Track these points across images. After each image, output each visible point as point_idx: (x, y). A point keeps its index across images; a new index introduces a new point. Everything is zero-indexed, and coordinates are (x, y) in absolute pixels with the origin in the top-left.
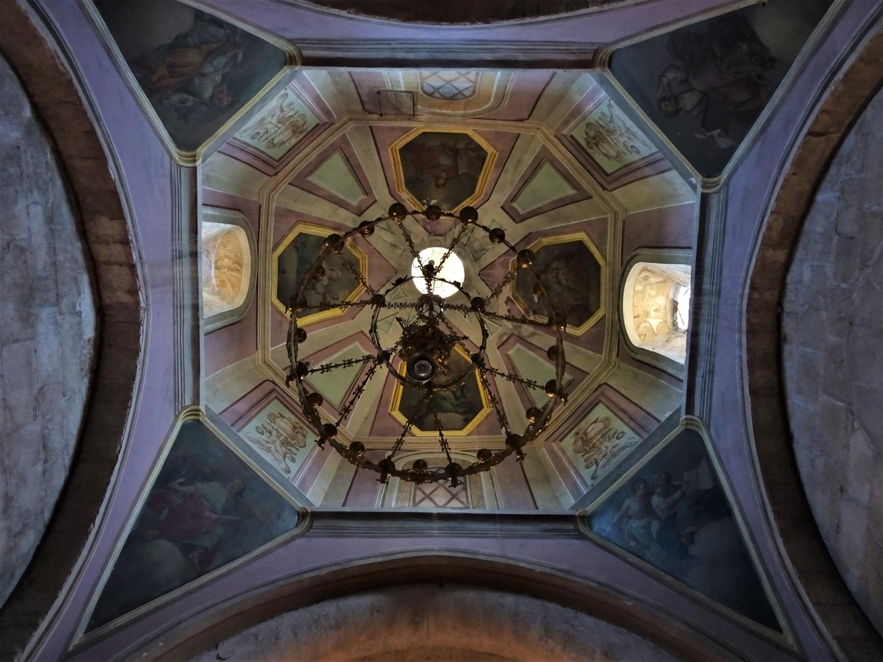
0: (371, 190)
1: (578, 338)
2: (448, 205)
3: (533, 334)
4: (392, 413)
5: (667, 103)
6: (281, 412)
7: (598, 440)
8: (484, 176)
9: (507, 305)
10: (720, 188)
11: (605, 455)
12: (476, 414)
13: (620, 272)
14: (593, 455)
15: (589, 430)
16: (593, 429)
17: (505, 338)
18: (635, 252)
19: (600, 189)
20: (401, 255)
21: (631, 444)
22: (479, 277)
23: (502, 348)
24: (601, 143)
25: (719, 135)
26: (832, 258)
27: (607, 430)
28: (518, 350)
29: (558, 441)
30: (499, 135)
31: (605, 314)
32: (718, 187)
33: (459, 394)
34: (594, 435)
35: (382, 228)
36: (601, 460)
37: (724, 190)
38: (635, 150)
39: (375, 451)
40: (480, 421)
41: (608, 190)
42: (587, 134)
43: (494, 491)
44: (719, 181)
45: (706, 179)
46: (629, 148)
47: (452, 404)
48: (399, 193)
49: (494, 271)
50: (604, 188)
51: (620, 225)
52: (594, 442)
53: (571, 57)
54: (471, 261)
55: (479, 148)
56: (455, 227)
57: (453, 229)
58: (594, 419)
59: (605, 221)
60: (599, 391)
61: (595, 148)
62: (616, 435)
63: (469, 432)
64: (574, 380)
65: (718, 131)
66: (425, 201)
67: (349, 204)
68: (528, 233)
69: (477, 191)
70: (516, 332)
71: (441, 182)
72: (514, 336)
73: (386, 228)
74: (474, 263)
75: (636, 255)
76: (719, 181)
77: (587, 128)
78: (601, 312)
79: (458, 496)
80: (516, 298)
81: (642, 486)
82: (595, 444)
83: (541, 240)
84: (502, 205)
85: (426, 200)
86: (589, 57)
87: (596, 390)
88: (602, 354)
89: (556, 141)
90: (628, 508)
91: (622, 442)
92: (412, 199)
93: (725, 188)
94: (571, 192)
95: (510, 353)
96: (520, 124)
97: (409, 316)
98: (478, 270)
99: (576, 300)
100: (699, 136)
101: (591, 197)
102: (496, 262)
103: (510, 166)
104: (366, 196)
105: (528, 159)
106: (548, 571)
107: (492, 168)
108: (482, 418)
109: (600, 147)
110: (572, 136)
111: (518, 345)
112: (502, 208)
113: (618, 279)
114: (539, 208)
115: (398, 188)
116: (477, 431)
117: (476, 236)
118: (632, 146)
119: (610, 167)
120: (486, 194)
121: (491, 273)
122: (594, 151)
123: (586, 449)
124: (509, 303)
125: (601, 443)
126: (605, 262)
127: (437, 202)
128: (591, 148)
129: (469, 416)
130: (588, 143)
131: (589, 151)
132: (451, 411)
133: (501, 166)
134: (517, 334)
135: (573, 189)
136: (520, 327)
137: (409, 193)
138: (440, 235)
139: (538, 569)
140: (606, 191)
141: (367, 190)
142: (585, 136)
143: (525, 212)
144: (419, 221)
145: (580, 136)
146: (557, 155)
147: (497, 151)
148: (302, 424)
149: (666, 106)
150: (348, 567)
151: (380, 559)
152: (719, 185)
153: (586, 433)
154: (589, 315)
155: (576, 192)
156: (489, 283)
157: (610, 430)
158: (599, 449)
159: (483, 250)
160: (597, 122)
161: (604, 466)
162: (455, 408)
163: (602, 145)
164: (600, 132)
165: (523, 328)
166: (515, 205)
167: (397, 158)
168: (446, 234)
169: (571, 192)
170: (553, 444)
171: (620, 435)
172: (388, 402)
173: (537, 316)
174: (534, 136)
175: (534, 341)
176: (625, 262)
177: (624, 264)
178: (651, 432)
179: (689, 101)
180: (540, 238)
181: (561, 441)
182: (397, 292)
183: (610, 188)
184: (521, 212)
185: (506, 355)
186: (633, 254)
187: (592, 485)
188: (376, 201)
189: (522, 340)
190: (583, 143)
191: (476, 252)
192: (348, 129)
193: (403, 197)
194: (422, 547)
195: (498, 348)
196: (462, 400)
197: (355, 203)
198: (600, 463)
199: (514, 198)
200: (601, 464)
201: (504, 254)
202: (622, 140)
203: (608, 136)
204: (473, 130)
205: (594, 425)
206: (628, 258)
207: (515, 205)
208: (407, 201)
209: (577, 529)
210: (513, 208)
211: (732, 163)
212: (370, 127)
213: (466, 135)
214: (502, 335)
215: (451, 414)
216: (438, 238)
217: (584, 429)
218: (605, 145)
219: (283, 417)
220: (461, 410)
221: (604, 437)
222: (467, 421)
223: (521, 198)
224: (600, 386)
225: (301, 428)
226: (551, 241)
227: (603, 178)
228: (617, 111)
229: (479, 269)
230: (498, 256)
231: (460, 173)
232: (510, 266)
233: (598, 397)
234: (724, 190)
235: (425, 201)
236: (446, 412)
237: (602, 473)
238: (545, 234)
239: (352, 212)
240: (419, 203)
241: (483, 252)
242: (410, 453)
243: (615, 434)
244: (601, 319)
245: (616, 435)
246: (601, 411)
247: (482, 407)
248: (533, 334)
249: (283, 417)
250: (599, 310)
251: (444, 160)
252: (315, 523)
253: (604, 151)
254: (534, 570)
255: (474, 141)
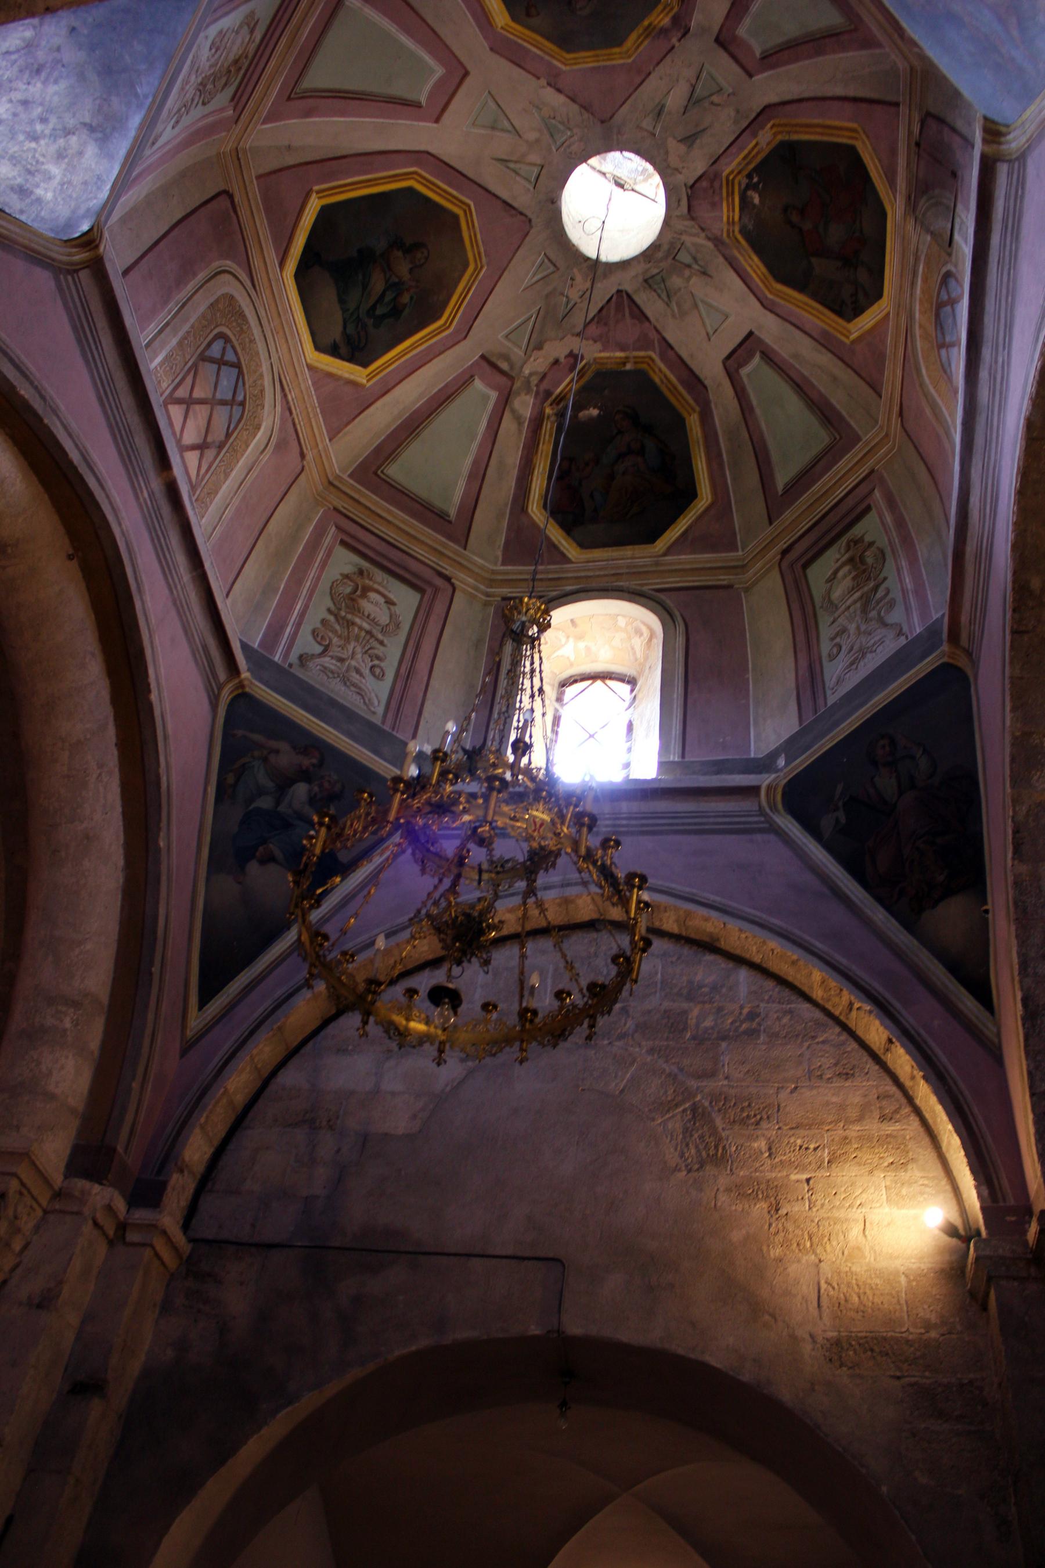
0: (772, 67)
1: (524, 510)
2: (750, 227)
3: (518, 419)
4: (314, 195)
5: (887, 749)
6: (260, 22)
7: (361, 628)
8: (806, 304)
9: (566, 357)
10: (765, 815)
11: (341, 660)
12: (350, 360)
13: (645, 588)
14: (335, 632)
15: (372, 595)
16: (377, 604)
17: (504, 366)
18: (679, 619)
19: (782, 545)
20: (641, 128)
21: (368, 704)
22: (614, 290)
23: (484, 364)
24: (854, 574)
25: (837, 820)
26: (666, 1004)
27: (380, 636)
28: (486, 398)
29: (341, 536)
30: (880, 358)
31: (572, 562)
32: (768, 810)
33: (379, 312)
34: (366, 614)
35: (694, 87)
36: (332, 657)
37: (762, 822)
38: (835, 650)
39: (232, 214)
40: (339, 373)
41: (781, 560)
42: (871, 544)
43: (232, 498)
44: (777, 811)
45: (780, 791)
46: (838, 640)
47: (358, 308)
48: (769, 126)
49: (628, 320)
50: (785, 552)
51: (724, 579)
52: (358, 621)
53: (964, 619)
54: (647, 270)
55: (858, 311)
56: (709, 239)
57: (703, 235)
58: (391, 596)
59: (732, 546)
60: (439, 582)
61: (847, 556)
62: (376, 662)
63: (316, 364)
64: (450, 522)
65: (843, 820)
66: (755, 180)
67: (739, 20)
68: (706, 382)
69: (779, 287)
70: (517, 384)
71: (795, 218)
72: (509, 383)
73: (696, 95)
74: (640, 279)
75: (674, 622)
76: (777, 811)
77: (878, 548)
78: (574, 553)
79: (206, 451)
80: (582, 373)
81: (314, 761)
82: (353, 624)
83: (694, 410)
84: (756, 333)
85: (758, 183)
86: (964, 641)
87: (440, 574)
88: (504, 564)
89: (864, 471)
90: (277, 752)
91: (369, 683)
92: (758, 153)
93: (766, 825)
94: (781, 480)
95: (478, 384)
96: (896, 409)
97: (516, 162)
98: (628, 287)
99: (592, 496)
100: (839, 788)
101: (771, 523)
102: (647, 324)
103: (824, 358)
104: (758, 54)
105: (838, 400)
106: (157, 713)
107: (826, 327)
108: (346, 375)
109: (846, 568)
110: (868, 509)
111: (494, 395)
112: (751, 334)
113: (633, 584)
114: (751, 409)
115: (779, 125)
116: (321, 377)
117: (694, 280)
118: (840, 647)
119: (818, 573)
120: (773, 303)
121: (624, 315)
122: (843, 551)
123: (340, 609)
124: (572, 360)
125: (357, 638)
126: (661, 552)
127: (754, 205)
128: (848, 550)
129: (344, 350)
130: (857, 542)
131: (844, 541)
132: (344, 311)
133: (826, 342)
134: (515, 387)
135: (786, 485)
136: (528, 391)
137: (771, 147)
138: (690, 208)
139: (154, 697)
140: (779, 557)
141: (772, 58)
142: (868, 539)
143: (745, 380)
144: (715, 166)
145: (869, 528)
146: (843, 464)
147: (853, 342)
148: (246, 65)
149: (884, 747)
150: (46, 421)
151: (74, 456)
152: (771, 810)
153: (366, 590)
154: (568, 528)
155: (780, 493)
156: (604, 312)
157: (382, 643)
158: (348, 640)
159: (668, 296)
160: (885, 579)
161: (325, 669)
162: (352, 314)
163: (850, 572)
164: (869, 579)
165: (528, 397)
166: (757, 359)
167: (838, 136)
168: (693, 219)
169: (781, 480)
170: (334, 528)
171: (377, 671)
172: (331, 176)
173: (553, 418)
174: (877, 422)
175: (508, 423)
176: (662, 596)
177: (658, 594)
178: (394, 733)
179: (886, 783)
180: (697, 409)
181: (343, 543)
182: (561, 127)
183: (785, 564)
184: (744, 371)
185: (472, 376)
186: (677, 614)
187: (290, 665)
188: (751, 76)
189: (505, 401)
190: (857, 531)
191: (664, 281)
192: (893, 57)
193: (761, 133)
194: (118, 500)
195: (483, 357)
196: (370, 322)
197: (742, 31)
198: (327, 659)
199: (769, 357)
200: (326, 661)
201: (664, 339)
202: (852, 628)
203: (861, 598)
204: (888, 314)
205: (382, 600)
206: (669, 603)
207: (757, 359)
208: (754, 143)
209: (220, 688)
210: (750, 356)
211: (798, 833)
212: (897, 104)
213: (879, 296)
214: (506, 357)
215: (338, 317)
216: (684, 202)
217: (371, 583)
218: (848, 582)
219: (252, 32)
220: (350, 329)
221: (368, 637)
222: (334, 351)
223: (769, 374)
224: (448, 579)
225: (240, 68)
226: (694, 432)
227: (798, 559)
228: (890, 646)
229: (630, 291)
230: (659, 327)
231: (814, 260)
232: (642, 354)
233: (429, 583)
234: (762, 822)
235: (755, 180)
236: (342, 301)
237: (312, 675)
238: (706, 417)
239: (722, 26)
240: (751, 166)
241: (664, 296)
242: (248, 284)
243: (378, 658)
244: (563, 555)
245: (376, 662)
246: (406, 600)
247: (365, 365)
248: (518, 419)
249: (252, 32)
250: (578, 549)
251: (835, 234)
252: (84, 275)
253: (840, 574)
254: (149, 691)
255: (872, 304)
